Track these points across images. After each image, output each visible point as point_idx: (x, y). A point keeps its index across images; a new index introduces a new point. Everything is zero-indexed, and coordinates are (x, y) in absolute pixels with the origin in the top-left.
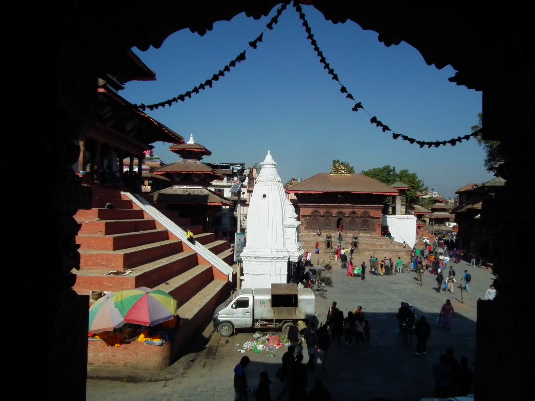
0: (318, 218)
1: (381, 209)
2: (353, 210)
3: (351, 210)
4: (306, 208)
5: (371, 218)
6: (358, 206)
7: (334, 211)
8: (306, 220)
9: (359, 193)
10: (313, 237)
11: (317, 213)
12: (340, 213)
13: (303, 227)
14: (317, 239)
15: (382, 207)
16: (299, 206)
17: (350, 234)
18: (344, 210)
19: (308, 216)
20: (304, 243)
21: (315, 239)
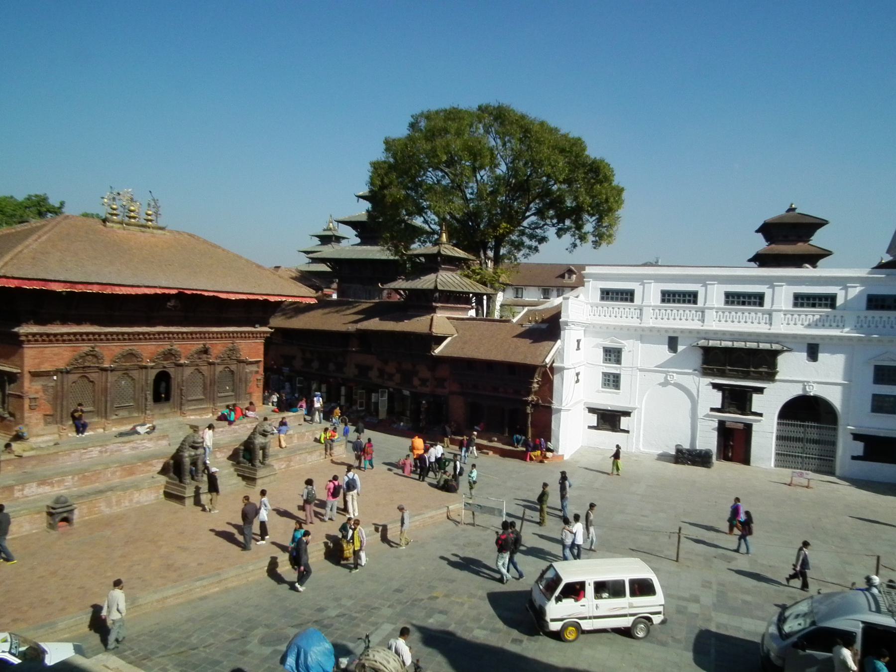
0: (93, 376)
1: (264, 337)
2: (204, 345)
3: (199, 345)
4: (51, 341)
5: (241, 364)
6: (213, 333)
7: (148, 350)
8: (51, 390)
9: (159, 291)
10: (99, 449)
11: (95, 360)
12: (169, 355)
13: (40, 416)
14: (112, 452)
15: (264, 332)
16: (23, 338)
17: (192, 417)
18: (177, 346)
19: (58, 372)
20: (80, 479)
21: (105, 455)
